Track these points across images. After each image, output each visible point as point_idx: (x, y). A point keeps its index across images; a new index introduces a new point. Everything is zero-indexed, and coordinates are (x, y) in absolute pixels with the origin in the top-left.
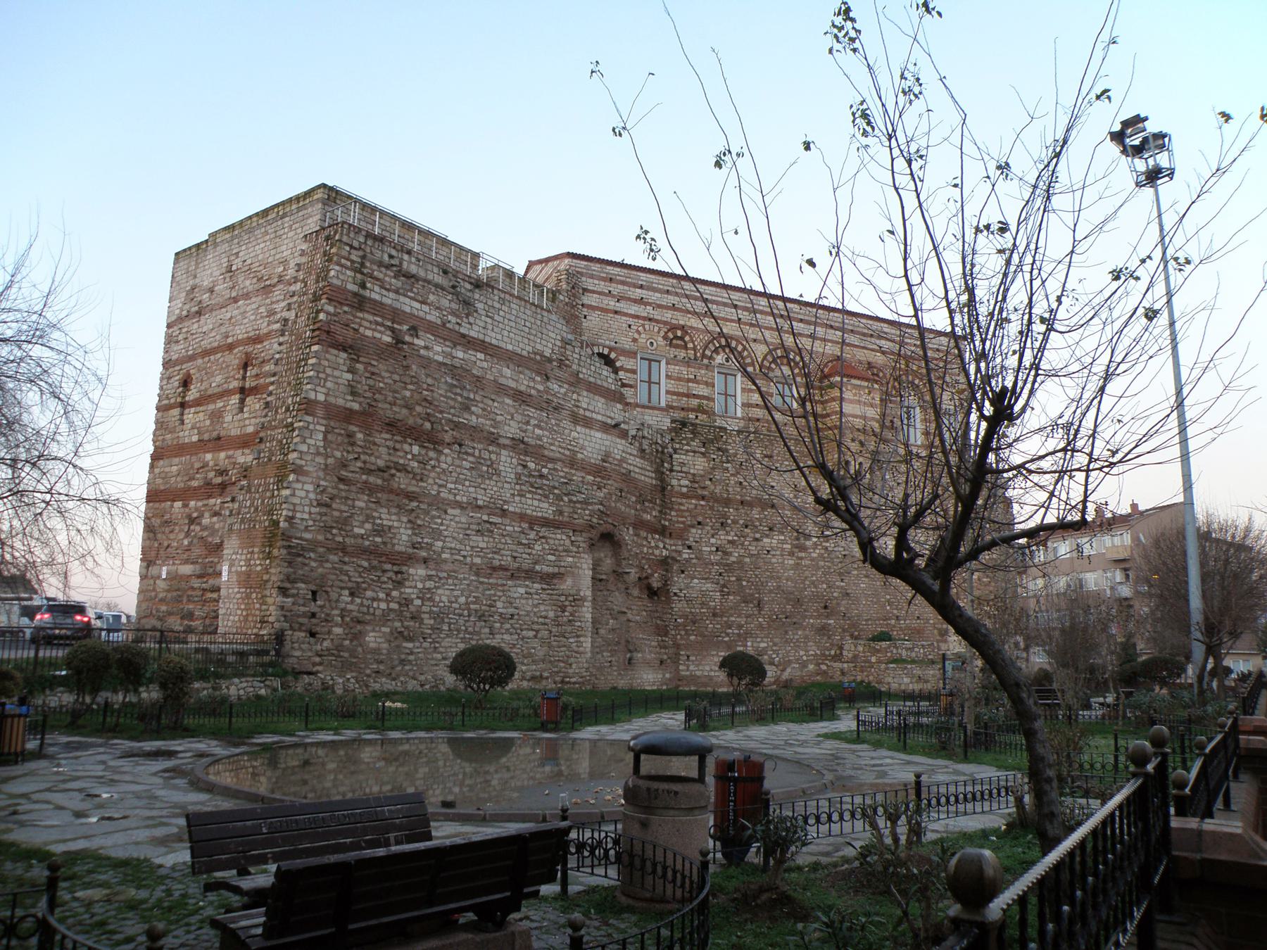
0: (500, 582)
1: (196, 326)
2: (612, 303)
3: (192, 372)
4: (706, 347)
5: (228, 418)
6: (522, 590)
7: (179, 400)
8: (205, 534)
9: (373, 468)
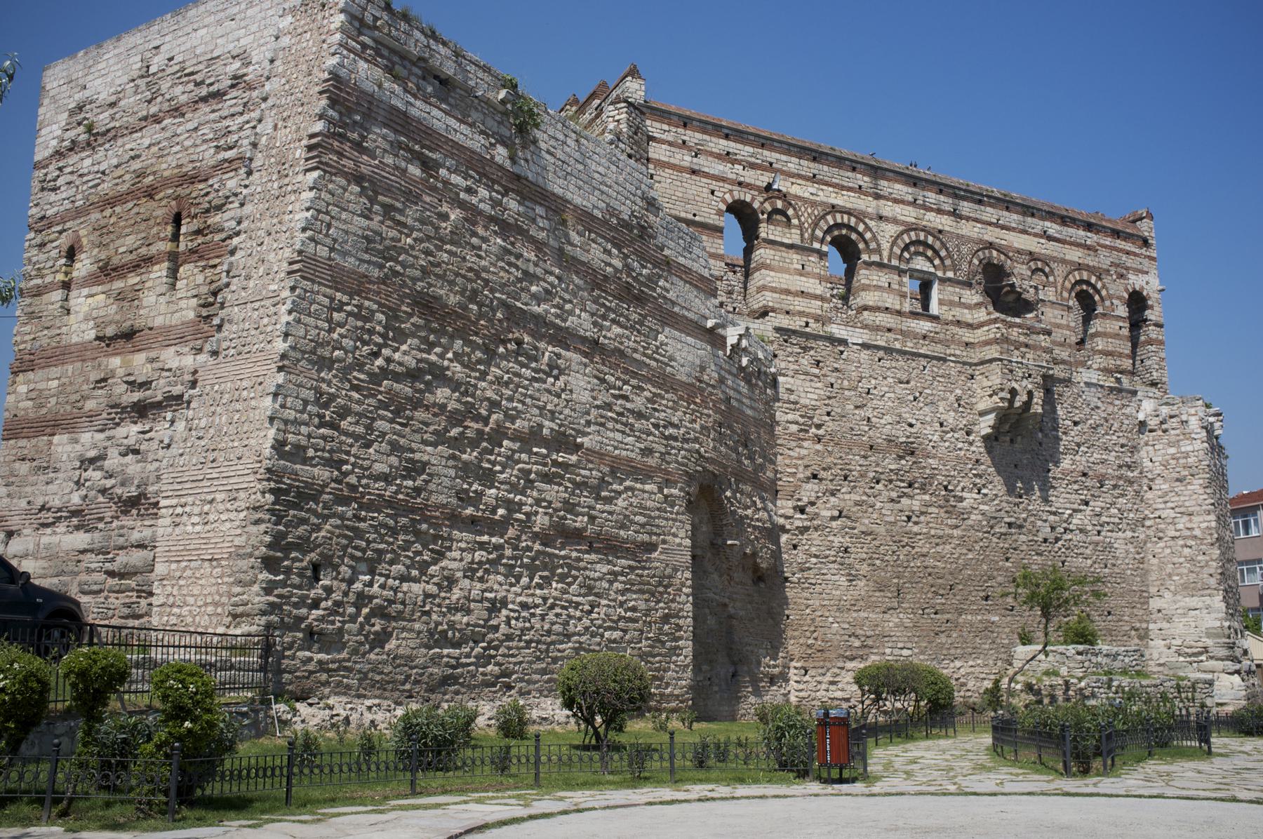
0: (574, 554)
1: (88, 162)
2: (688, 158)
3: (82, 233)
4: (816, 225)
5: (149, 299)
6: (605, 568)
7: (60, 277)
8: (109, 483)
9: (399, 369)
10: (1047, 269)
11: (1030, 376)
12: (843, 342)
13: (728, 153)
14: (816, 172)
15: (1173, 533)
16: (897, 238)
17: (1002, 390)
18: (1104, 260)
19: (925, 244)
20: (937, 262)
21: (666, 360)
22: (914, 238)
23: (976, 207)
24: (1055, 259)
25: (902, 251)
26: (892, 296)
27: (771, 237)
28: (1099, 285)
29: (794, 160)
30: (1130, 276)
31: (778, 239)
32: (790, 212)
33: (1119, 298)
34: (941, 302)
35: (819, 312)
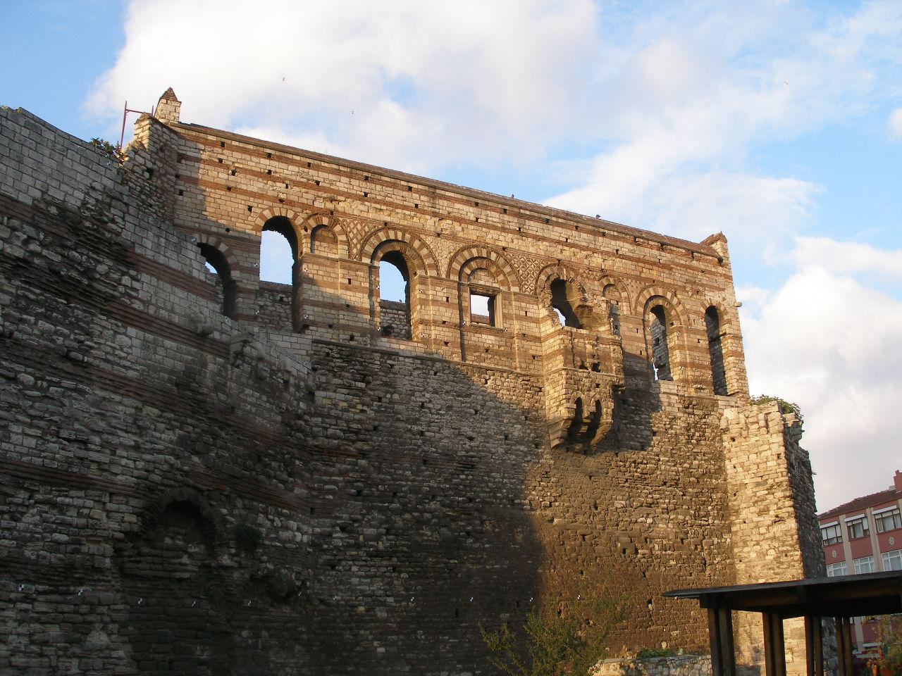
2: (223, 176)
4: (366, 241)
11: (598, 386)
13: (270, 172)
14: (367, 191)
18: (678, 277)
21: (128, 364)
22: (476, 255)
24: (628, 276)
34: (505, 317)
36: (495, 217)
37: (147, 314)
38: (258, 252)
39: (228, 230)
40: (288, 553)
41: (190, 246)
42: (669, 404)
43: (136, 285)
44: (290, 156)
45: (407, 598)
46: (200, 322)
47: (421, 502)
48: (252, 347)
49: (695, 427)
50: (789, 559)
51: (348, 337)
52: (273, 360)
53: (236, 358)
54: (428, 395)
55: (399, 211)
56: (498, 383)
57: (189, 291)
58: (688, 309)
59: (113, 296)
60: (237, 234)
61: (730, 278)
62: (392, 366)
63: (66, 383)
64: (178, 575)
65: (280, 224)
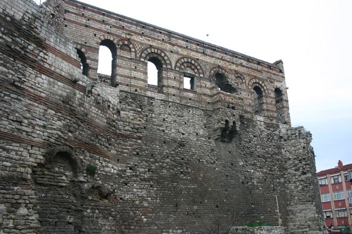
2: (84, 21)
4: (142, 52)
10: (242, 77)
12: (152, 98)
15: (294, 180)
16: (178, 60)
17: (222, 120)
18: (264, 76)
19: (191, 63)
20: (196, 71)
21: (41, 90)
22: (186, 61)
23: (214, 52)
24: (245, 74)
25: (181, 65)
26: (175, 82)
27: (122, 55)
28: (263, 85)
29: (135, 27)
30: (275, 83)
31: (125, 56)
32: (131, 46)
33: (271, 90)
35: (142, 86)
36: (194, 46)
37: (51, 70)
38: (98, 53)
39: (86, 43)
40: (108, 177)
41: (70, 44)
42: (260, 125)
43: (46, 57)
44: (112, 15)
45: (156, 198)
46: (74, 76)
47: (163, 158)
48: (95, 90)
49: (270, 135)
50: (308, 189)
51: (134, 90)
52: (103, 96)
53: (88, 93)
54: (166, 115)
55: (156, 41)
56: (194, 112)
57: (69, 63)
58: (269, 88)
59: (35, 60)
60: (89, 45)
61: (284, 77)
62: (152, 103)
63: (12, 95)
64: (61, 184)
65: (107, 43)
